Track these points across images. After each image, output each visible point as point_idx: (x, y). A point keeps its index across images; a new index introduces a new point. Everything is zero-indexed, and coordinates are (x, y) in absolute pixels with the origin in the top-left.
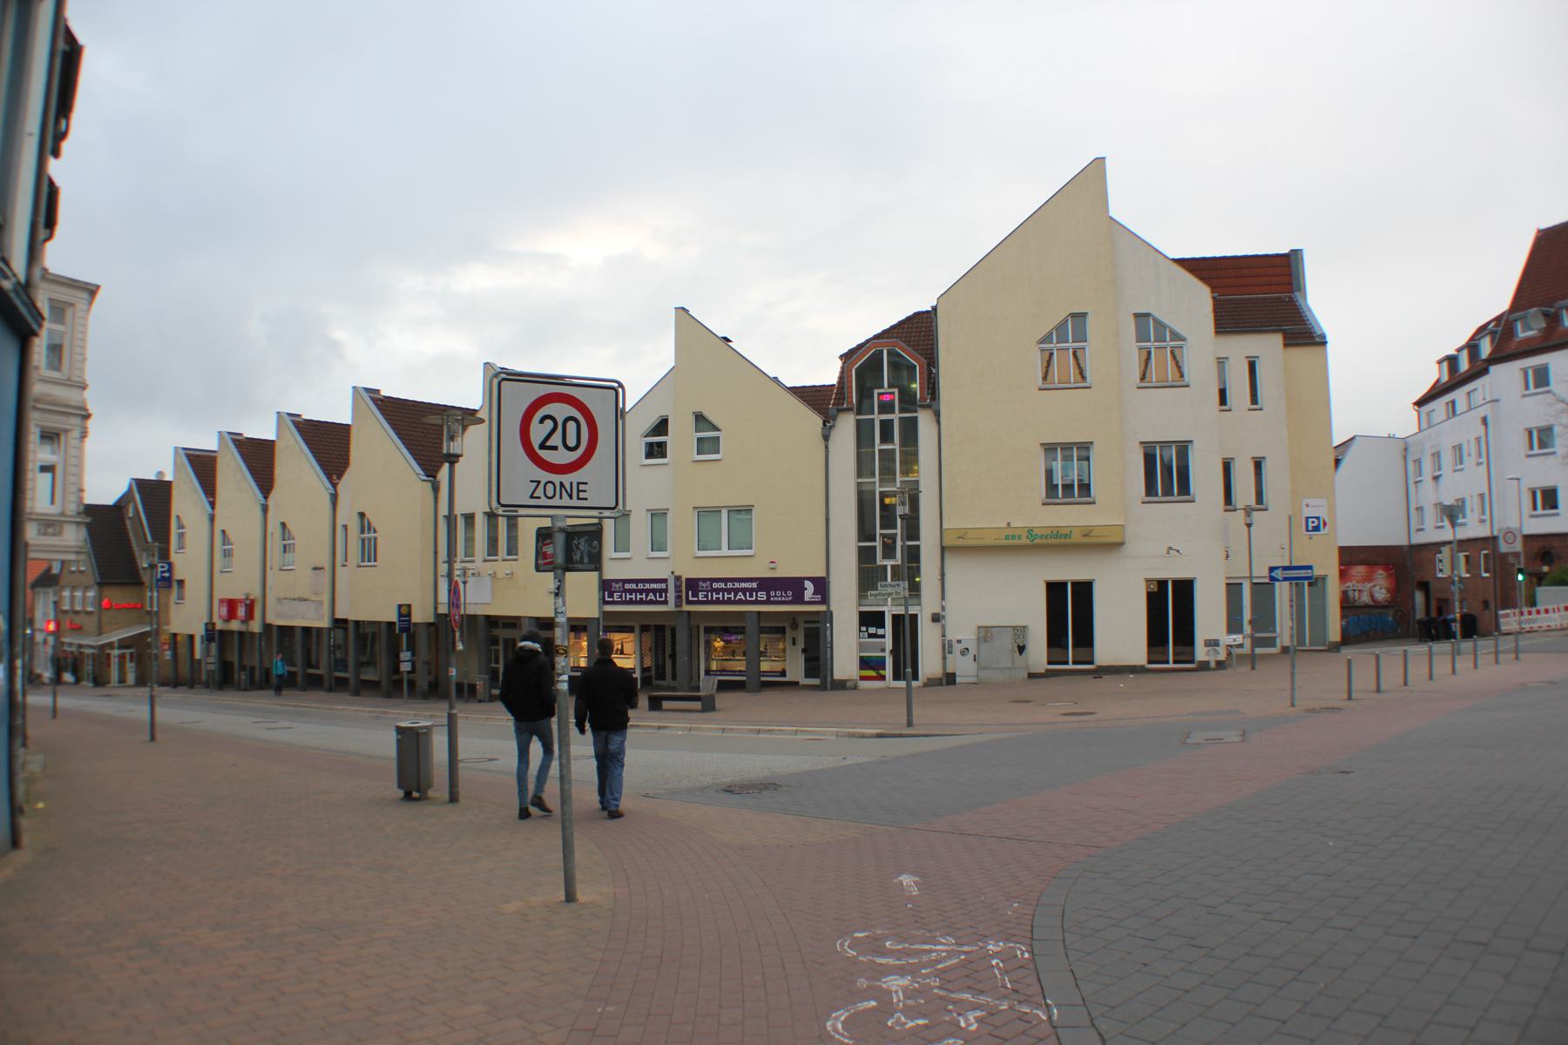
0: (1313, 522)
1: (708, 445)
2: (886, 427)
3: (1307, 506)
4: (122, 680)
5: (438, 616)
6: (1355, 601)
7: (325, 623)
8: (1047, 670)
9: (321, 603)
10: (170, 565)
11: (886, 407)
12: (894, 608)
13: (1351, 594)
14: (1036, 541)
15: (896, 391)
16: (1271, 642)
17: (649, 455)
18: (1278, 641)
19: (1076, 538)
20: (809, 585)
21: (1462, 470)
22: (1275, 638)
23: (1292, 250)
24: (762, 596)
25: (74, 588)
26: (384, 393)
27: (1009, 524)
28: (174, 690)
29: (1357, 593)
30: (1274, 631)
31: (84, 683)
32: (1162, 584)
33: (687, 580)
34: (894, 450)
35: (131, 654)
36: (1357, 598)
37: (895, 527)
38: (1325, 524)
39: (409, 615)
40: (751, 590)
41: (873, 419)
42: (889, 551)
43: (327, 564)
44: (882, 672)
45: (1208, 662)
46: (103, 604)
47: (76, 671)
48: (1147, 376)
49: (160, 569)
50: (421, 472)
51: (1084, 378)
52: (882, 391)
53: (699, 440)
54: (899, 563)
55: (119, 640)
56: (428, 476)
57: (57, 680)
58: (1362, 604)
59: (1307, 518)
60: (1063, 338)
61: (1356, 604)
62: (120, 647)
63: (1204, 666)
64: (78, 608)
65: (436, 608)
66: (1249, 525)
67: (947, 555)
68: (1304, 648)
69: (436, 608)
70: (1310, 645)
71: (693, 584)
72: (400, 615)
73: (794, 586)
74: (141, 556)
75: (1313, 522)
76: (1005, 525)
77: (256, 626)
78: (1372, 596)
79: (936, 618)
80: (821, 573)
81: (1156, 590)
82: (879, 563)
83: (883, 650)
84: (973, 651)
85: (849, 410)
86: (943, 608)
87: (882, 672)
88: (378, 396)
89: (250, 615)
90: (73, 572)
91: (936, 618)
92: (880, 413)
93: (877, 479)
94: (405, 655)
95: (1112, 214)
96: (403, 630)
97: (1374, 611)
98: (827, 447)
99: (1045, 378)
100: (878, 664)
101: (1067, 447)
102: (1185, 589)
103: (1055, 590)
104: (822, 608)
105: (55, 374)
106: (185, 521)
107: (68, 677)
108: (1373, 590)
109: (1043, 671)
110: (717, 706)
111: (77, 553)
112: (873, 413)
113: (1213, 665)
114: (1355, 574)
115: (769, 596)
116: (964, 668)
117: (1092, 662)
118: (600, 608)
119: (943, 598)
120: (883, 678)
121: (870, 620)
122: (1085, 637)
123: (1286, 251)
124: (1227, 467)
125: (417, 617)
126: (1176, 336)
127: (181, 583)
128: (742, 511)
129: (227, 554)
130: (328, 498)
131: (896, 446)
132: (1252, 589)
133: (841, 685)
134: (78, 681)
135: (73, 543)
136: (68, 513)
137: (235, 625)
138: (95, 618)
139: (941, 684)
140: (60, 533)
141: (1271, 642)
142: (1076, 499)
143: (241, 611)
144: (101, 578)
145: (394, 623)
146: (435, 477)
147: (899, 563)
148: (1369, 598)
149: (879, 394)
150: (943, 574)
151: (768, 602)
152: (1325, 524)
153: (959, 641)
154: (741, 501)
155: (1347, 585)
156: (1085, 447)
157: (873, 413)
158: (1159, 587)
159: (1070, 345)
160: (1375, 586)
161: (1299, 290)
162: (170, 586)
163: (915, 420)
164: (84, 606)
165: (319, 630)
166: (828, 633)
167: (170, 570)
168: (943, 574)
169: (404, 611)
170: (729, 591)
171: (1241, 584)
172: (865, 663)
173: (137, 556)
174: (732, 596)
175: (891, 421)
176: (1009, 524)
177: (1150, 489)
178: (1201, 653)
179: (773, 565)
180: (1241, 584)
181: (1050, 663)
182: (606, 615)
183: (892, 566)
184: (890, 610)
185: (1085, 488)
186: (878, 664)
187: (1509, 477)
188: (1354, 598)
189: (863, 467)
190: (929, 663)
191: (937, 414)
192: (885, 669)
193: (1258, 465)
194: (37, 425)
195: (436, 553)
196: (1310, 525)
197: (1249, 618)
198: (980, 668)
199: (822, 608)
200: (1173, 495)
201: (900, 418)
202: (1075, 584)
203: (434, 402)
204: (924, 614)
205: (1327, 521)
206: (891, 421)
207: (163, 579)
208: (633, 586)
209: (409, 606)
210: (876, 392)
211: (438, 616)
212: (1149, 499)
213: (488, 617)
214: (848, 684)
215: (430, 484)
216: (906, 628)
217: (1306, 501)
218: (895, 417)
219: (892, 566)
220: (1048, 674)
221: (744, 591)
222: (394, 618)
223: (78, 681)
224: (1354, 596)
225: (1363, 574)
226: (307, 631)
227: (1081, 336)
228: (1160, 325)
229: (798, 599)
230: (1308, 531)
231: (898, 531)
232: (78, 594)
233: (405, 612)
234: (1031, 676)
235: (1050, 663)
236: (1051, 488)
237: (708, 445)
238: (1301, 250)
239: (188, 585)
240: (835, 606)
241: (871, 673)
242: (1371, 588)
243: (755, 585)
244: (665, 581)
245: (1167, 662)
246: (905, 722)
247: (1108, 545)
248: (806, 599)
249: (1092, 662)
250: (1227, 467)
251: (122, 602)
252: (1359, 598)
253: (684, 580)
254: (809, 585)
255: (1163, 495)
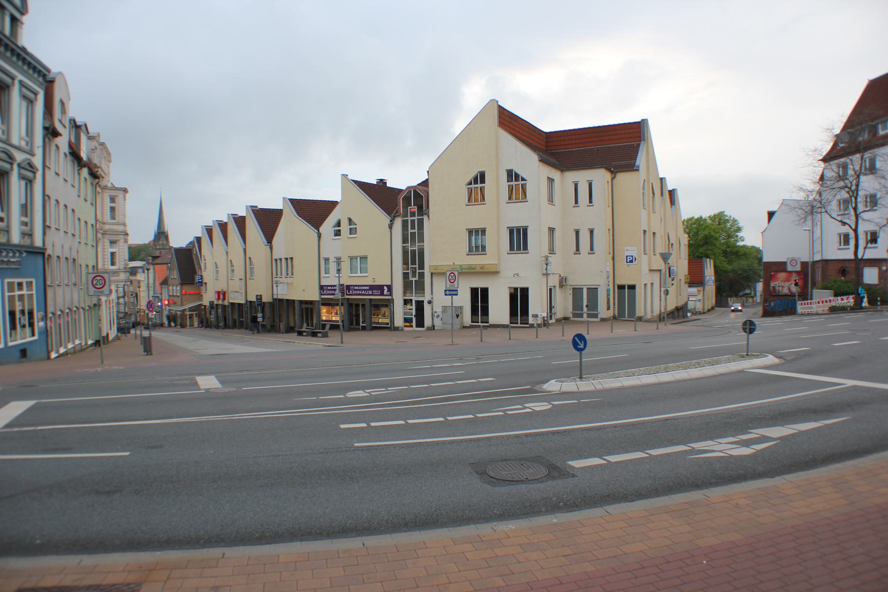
0: (630, 258)
1: (353, 231)
2: (413, 222)
3: (627, 250)
4: (192, 325)
5: (273, 299)
6: (779, 292)
7: (243, 302)
8: (471, 325)
9: (242, 293)
10: (201, 276)
11: (413, 215)
12: (416, 298)
13: (777, 288)
14: (463, 271)
15: (416, 207)
16: (596, 316)
17: (336, 235)
18: (599, 315)
19: (478, 269)
20: (385, 288)
21: (292, 277)
22: (597, 314)
23: (642, 120)
24: (370, 292)
25: (173, 285)
26: (260, 207)
27: (454, 263)
28: (206, 329)
29: (781, 288)
30: (597, 311)
31: (178, 327)
32: (516, 289)
33: (346, 285)
34: (415, 232)
35: (196, 314)
36: (780, 290)
37: (416, 265)
38: (635, 259)
39: (261, 299)
40: (367, 290)
41: (408, 220)
42: (414, 276)
43: (243, 277)
44: (412, 324)
45: (533, 324)
46: (183, 292)
47: (175, 322)
48: (512, 199)
49: (197, 278)
50: (266, 242)
51: (484, 200)
52: (411, 207)
53: (350, 229)
54: (417, 279)
55: (189, 308)
56: (268, 243)
57: (170, 325)
58: (784, 294)
59: (627, 256)
60: (476, 183)
61: (780, 294)
62: (190, 311)
63: (532, 326)
64: (175, 294)
65: (273, 296)
66: (547, 264)
67: (433, 276)
68: (625, 319)
69: (273, 296)
70: (628, 318)
71: (348, 287)
72: (257, 299)
73: (380, 288)
74: (199, 271)
75: (630, 258)
76: (452, 264)
77: (226, 303)
78: (789, 290)
79: (430, 302)
80: (389, 283)
81: (513, 292)
82: (410, 279)
83: (412, 315)
84: (441, 317)
85: (398, 216)
86: (432, 298)
87: (412, 324)
88: (256, 209)
89: (224, 299)
90: (172, 278)
91: (430, 302)
92: (410, 217)
93: (409, 245)
94: (260, 315)
95: (152, 238)
96: (258, 305)
97: (791, 298)
98: (391, 232)
99: (469, 200)
100: (410, 320)
101: (477, 231)
102: (525, 291)
103: (474, 291)
104: (390, 297)
105: (113, 221)
106: (206, 258)
107: (173, 324)
108: (790, 286)
109: (469, 326)
110: (329, 335)
111: (125, 282)
112: (418, 216)
113: (535, 325)
114: (779, 277)
115: (373, 292)
116: (438, 323)
117: (488, 322)
118: (320, 297)
119: (432, 294)
120: (412, 326)
121: (406, 302)
122: (485, 311)
123: (639, 120)
124: (577, 232)
125: (264, 300)
126: (523, 179)
127: (206, 283)
128: (364, 258)
129: (233, 271)
130: (242, 250)
131: (416, 231)
132: (587, 291)
133: (397, 329)
134: (176, 326)
135: (124, 279)
136: (121, 268)
137: (220, 302)
138: (180, 298)
139: (431, 330)
140: (119, 275)
141: (596, 316)
142: (480, 253)
143: (221, 296)
144: (181, 281)
145: (255, 302)
146: (271, 243)
147: (417, 279)
148: (788, 291)
149: (410, 209)
150: (432, 284)
151: (372, 295)
152: (635, 259)
153: (436, 312)
154: (363, 254)
155: (775, 283)
156: (483, 231)
157: (408, 217)
158: (514, 291)
159: (479, 185)
160: (791, 284)
161: (644, 140)
162: (202, 285)
163: (423, 219)
164: (176, 293)
165: (242, 304)
166: (392, 307)
167: (202, 279)
168: (432, 284)
169: (259, 297)
170: (360, 290)
171: (597, 288)
172: (406, 320)
173: (197, 271)
174: (361, 292)
175: (415, 220)
176: (454, 263)
177: (512, 248)
178: (531, 320)
179: (374, 280)
180: (582, 288)
181: (472, 322)
182: (322, 299)
183: (415, 280)
184: (414, 298)
185: (484, 248)
186: (410, 320)
187: (804, 229)
188: (779, 290)
189: (405, 241)
190: (428, 322)
191: (429, 217)
192: (412, 323)
193: (592, 232)
194: (108, 240)
195: (272, 274)
196: (628, 260)
197: (586, 304)
198: (443, 323)
199: (390, 297)
200: (521, 250)
201: (418, 219)
202: (481, 289)
203: (311, 199)
204: (426, 299)
205: (636, 258)
206: (415, 220)
207: (199, 282)
208: (357, 288)
209: (261, 295)
210: (409, 208)
211: (273, 299)
212: (511, 252)
213: (288, 300)
214: (400, 328)
215: (269, 246)
216: (420, 306)
217: (626, 248)
218: (416, 218)
219: (415, 280)
220: (471, 327)
221: (364, 290)
222: (255, 300)
223: (176, 326)
224: (779, 290)
225: (785, 277)
226: (239, 304)
227: (483, 181)
228: (517, 176)
229: (382, 294)
230: (627, 262)
231: (417, 266)
232: (174, 288)
233: (259, 298)
234: (464, 327)
235: (472, 322)
236: (470, 250)
237: (353, 231)
238: (647, 120)
239: (208, 284)
240: (395, 296)
241: (408, 324)
242: (789, 285)
243: (368, 288)
244: (335, 286)
245: (518, 324)
246: (340, 341)
247: (494, 273)
248: (385, 294)
249: (488, 322)
250: (577, 232)
251: (191, 291)
252: (782, 291)
253: (345, 286)
254: (385, 288)
255: (523, 250)
